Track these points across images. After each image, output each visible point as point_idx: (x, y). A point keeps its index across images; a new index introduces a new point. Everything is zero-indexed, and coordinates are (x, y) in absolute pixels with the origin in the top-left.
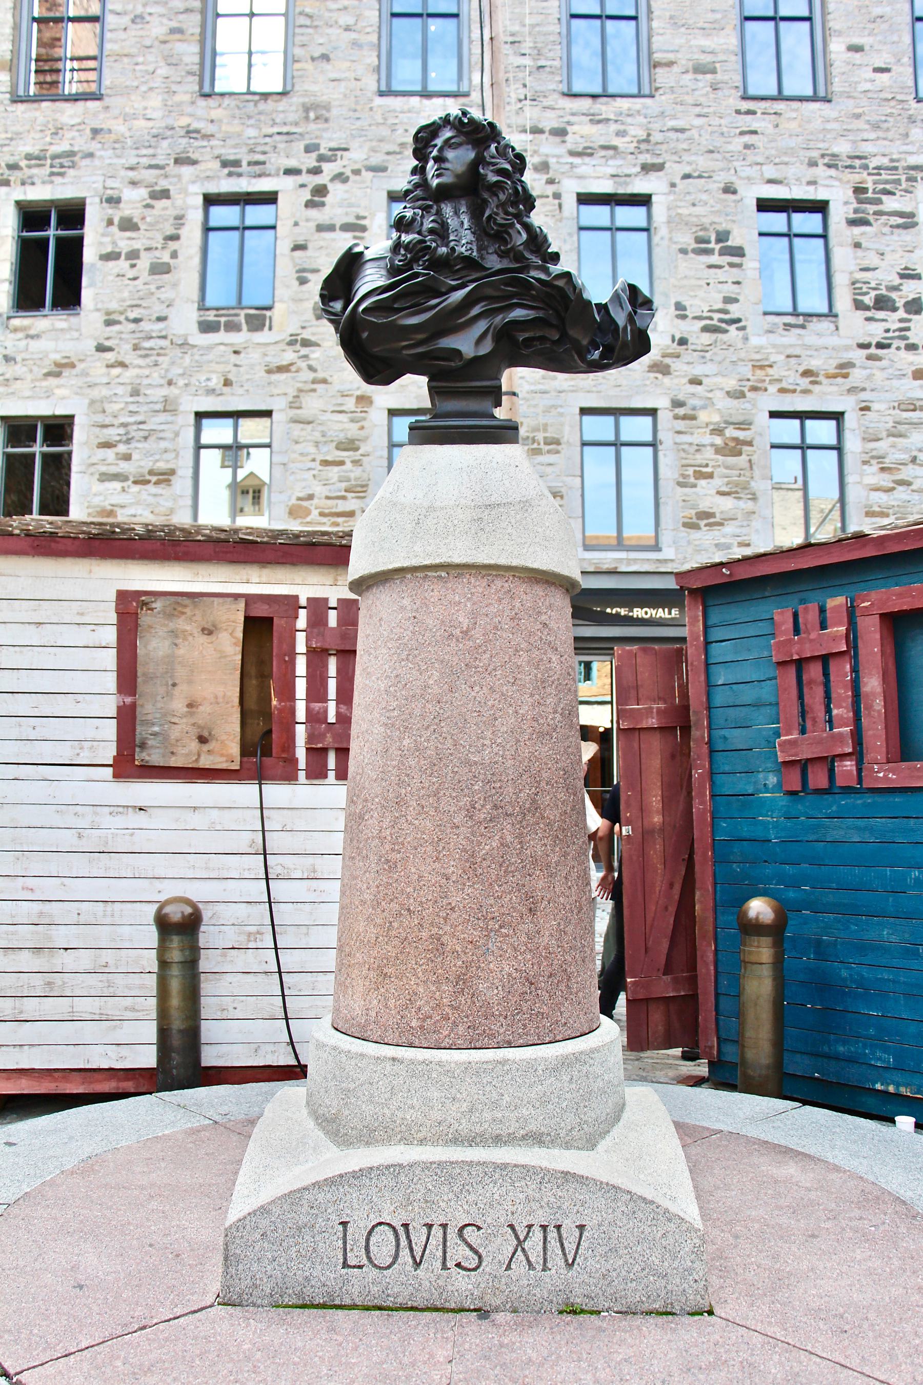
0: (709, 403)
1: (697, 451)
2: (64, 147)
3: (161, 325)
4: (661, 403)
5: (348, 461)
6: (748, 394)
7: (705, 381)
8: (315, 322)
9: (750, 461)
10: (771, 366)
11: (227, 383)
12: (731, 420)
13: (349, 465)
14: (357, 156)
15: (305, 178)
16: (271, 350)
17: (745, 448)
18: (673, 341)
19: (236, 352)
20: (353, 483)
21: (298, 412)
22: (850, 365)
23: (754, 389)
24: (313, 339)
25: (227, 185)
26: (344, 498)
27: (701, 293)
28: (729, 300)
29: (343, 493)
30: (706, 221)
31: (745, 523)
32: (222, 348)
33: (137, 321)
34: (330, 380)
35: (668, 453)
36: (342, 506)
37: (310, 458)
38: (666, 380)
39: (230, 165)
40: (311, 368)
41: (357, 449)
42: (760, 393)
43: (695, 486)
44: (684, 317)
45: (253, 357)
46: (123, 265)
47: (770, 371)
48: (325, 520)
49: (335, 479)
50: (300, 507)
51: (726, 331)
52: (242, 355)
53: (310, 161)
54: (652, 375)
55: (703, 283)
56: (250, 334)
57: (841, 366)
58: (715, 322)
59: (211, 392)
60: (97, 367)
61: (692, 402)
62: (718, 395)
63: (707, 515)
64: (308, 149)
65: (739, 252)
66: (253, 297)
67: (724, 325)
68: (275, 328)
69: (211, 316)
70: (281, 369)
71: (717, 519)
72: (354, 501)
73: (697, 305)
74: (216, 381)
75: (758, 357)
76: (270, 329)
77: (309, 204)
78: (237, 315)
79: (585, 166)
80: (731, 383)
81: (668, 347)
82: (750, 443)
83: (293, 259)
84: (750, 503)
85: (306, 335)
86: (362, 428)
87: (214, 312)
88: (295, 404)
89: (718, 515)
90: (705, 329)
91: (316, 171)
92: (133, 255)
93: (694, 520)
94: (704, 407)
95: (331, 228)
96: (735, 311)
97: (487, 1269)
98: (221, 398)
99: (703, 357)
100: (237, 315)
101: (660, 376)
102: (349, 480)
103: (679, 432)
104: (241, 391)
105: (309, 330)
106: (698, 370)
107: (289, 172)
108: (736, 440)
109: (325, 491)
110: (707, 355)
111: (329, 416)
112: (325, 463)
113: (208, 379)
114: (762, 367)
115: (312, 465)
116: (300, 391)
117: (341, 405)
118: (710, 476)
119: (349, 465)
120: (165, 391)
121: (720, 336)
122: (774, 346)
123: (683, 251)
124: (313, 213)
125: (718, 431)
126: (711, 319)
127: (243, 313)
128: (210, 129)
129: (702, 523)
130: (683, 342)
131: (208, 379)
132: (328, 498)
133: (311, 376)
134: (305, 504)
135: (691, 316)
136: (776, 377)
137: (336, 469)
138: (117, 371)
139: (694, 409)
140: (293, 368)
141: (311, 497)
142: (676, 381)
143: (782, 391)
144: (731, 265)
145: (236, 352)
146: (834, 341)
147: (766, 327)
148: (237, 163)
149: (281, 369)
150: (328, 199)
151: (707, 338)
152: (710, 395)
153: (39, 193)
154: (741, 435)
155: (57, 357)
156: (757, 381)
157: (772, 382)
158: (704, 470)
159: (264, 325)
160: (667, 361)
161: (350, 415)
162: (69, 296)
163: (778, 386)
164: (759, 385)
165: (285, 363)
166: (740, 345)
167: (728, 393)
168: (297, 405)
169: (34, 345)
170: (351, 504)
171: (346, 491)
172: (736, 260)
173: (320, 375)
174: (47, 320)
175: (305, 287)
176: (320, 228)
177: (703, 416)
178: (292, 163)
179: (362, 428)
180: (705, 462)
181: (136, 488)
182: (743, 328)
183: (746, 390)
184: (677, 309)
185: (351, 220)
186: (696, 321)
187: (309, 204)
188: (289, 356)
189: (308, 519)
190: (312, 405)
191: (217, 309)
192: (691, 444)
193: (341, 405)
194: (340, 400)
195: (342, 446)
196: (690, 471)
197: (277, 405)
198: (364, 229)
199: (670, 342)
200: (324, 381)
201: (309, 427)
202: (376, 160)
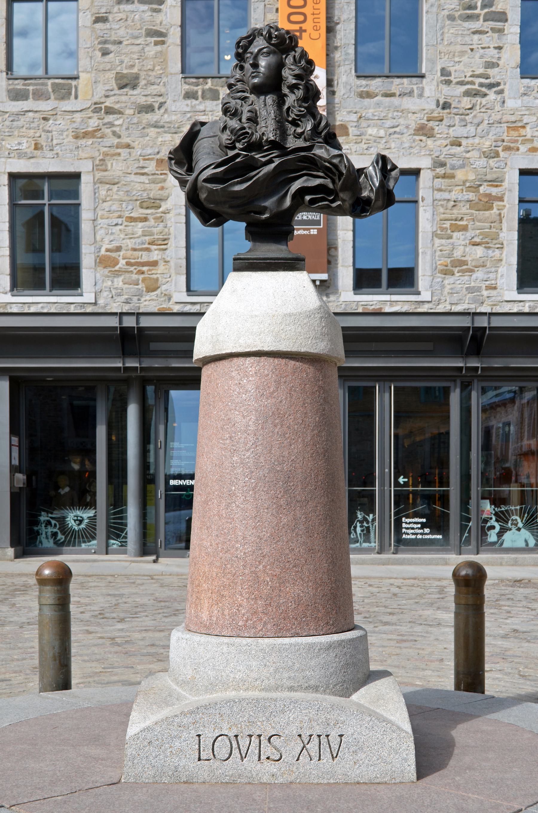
1: (454, 206)
5: (151, 217)
6: (502, 154)
7: (464, 142)
8: (117, 92)
9: (500, 214)
10: (523, 127)
12: (489, 177)
13: (152, 222)
16: (78, 117)
17: (496, 204)
18: (438, 106)
19: (45, 119)
20: (156, 237)
21: (105, 173)
23: (507, 149)
24: (117, 106)
26: (148, 250)
29: (146, 246)
31: (493, 269)
32: (31, 114)
34: (132, 144)
35: (427, 208)
36: (145, 257)
37: (116, 214)
38: (430, 142)
40: (114, 133)
41: (160, 207)
42: (513, 152)
43: (451, 237)
44: (448, 82)
47: (522, 132)
48: (132, 269)
49: (140, 233)
50: (109, 257)
51: (485, 95)
52: (51, 122)
54: (417, 138)
55: (467, 48)
56: (57, 102)
58: (476, 87)
63: (461, 263)
66: (57, 66)
67: (484, 89)
68: (80, 97)
69: (19, 85)
70: (86, 135)
71: (469, 267)
72: (156, 252)
73: (458, 72)
74: (26, 146)
75: (513, 118)
76: (76, 97)
78: (43, 84)
81: (433, 111)
82: (501, 199)
83: (93, 30)
84: (497, 252)
85: (109, 103)
86: (162, 188)
87: (22, 82)
88: (101, 165)
89: (469, 263)
90: (467, 93)
93: (449, 267)
94: (463, 166)
97: (286, 760)
98: (32, 160)
99: (464, 120)
100: (43, 84)
101: (424, 138)
102: (152, 234)
103: (440, 190)
104: (50, 154)
105: (112, 99)
106: (458, 131)
108: (489, 195)
109: (130, 244)
110: (467, 117)
111: (133, 177)
113: (19, 144)
115: (120, 221)
116: (106, 154)
117: (143, 167)
118: (465, 228)
119: (152, 222)
121: (479, 99)
122: (528, 108)
125: (475, 188)
126: (473, 83)
127: (50, 82)
129: (456, 270)
130: (446, 106)
131: (19, 144)
132: (135, 250)
133: (116, 141)
134: (114, 255)
135: (455, 81)
136: (529, 137)
137: (140, 225)
139: (453, 168)
140: (99, 134)
142: (438, 143)
144: (493, 30)
145: (45, 119)
147: (522, 90)
151: (466, 102)
152: (468, 155)
156: (509, 141)
157: (524, 142)
158: (461, 223)
159: (70, 94)
160: (431, 124)
161: (150, 177)
163: (529, 146)
164: (512, 145)
165: (90, 129)
166: (498, 108)
167: (484, 153)
168: (103, 167)
170: (155, 256)
171: (149, 244)
175: (107, 58)
179: (162, 188)
180: (460, 216)
182: (501, 92)
183: (500, 149)
184: (442, 75)
186: (459, 86)
188: (94, 123)
189: (117, 268)
190: (116, 168)
191: (25, 79)
192: (449, 200)
193: (143, 167)
194: (142, 163)
195: (145, 205)
196: (447, 224)
197: (84, 167)
199: (434, 106)
200: (128, 146)
201: (115, 188)
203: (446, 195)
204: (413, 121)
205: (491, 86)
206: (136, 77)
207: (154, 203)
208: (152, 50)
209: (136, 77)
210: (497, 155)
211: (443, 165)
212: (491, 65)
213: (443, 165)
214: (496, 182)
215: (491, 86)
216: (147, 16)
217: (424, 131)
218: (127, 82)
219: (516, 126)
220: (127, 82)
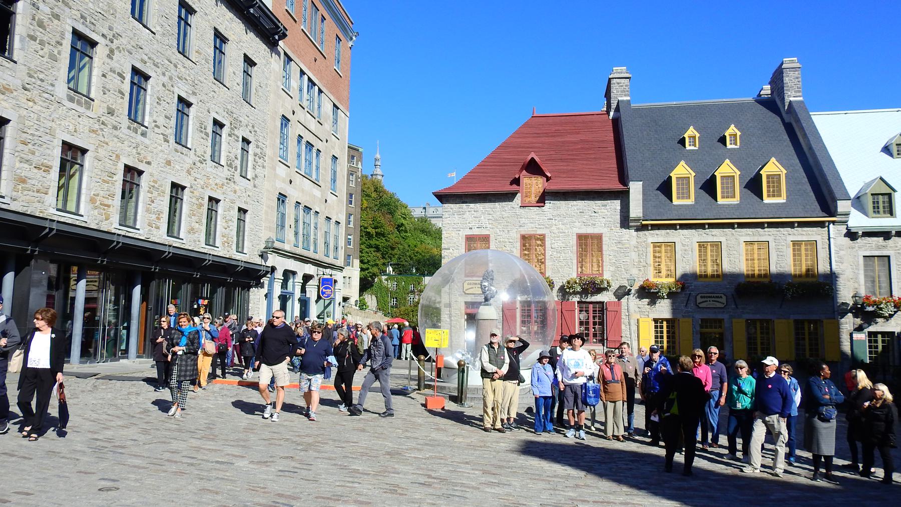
3: (50, 88)
14: (122, 41)
33: (42, 80)
46: (35, 45)
60: (22, 96)
64: (111, 29)
65: (207, 134)
79: (181, 84)
92: (42, 43)
107: (103, 35)
112: (104, 181)
120: (50, 124)
124: (109, 61)
138: (31, 104)
178: (105, 33)
181: (36, 171)
190: (102, 153)
202: (129, 47)
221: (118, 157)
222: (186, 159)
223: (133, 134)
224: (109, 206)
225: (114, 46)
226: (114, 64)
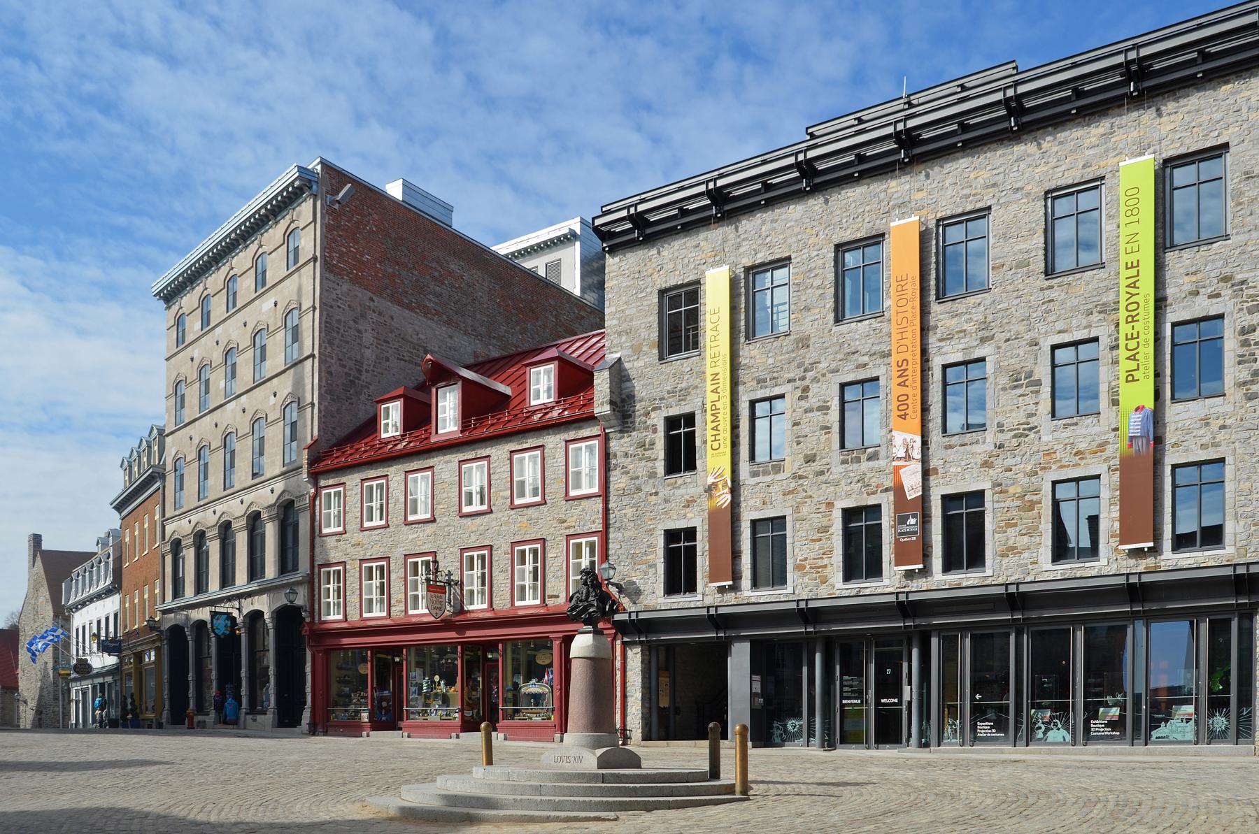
0: (1015, 482)
2: (684, 385)
4: (985, 485)
11: (764, 503)
15: (798, 383)
22: (1107, 443)
25: (760, 394)
27: (1013, 414)
28: (1031, 415)
30: (1018, 367)
39: (761, 381)
44: (1002, 431)
45: (775, 489)
53: (800, 372)
57: (1100, 445)
59: (756, 509)
61: (1004, 483)
62: (1021, 475)
70: (789, 493)
77: (801, 398)
80: (1029, 467)
88: (796, 510)
90: (1015, 436)
91: (803, 378)
95: (811, 410)
96: (1033, 421)
106: (1010, 462)
107: (789, 381)
112: (813, 541)
114: (1048, 455)
123: (1004, 389)
128: (752, 362)
141: (806, 559)
143: (1062, 467)
146: (1096, 429)
148: (765, 381)
149: (789, 493)
150: (810, 394)
151: (1015, 442)
153: (674, 412)
154: (1035, 498)
155: (687, 497)
162: (691, 466)
169: (678, 492)
172: (1036, 388)
173: (809, 493)
174: (683, 478)
176: (806, 411)
177: (1011, 490)
178: (791, 375)
185: (821, 404)
187: (801, 398)
188: (793, 485)
190: (805, 510)
197: (787, 512)
198: (828, 408)
203: (1002, 505)
204: (979, 460)
205: (1030, 429)
206: (815, 455)
207: (824, 530)
208: (823, 438)
209: (815, 455)
210: (1036, 473)
211: (1000, 485)
212: (1031, 415)
213: (1000, 485)
214: (1036, 491)
215: (1030, 429)
216: (821, 418)
217: (987, 464)
218: (810, 459)
219: (1048, 453)
220: (810, 459)
221: (830, 505)
222: (976, 448)
223: (855, 466)
224: (825, 566)
225: (806, 382)
226: (813, 401)
